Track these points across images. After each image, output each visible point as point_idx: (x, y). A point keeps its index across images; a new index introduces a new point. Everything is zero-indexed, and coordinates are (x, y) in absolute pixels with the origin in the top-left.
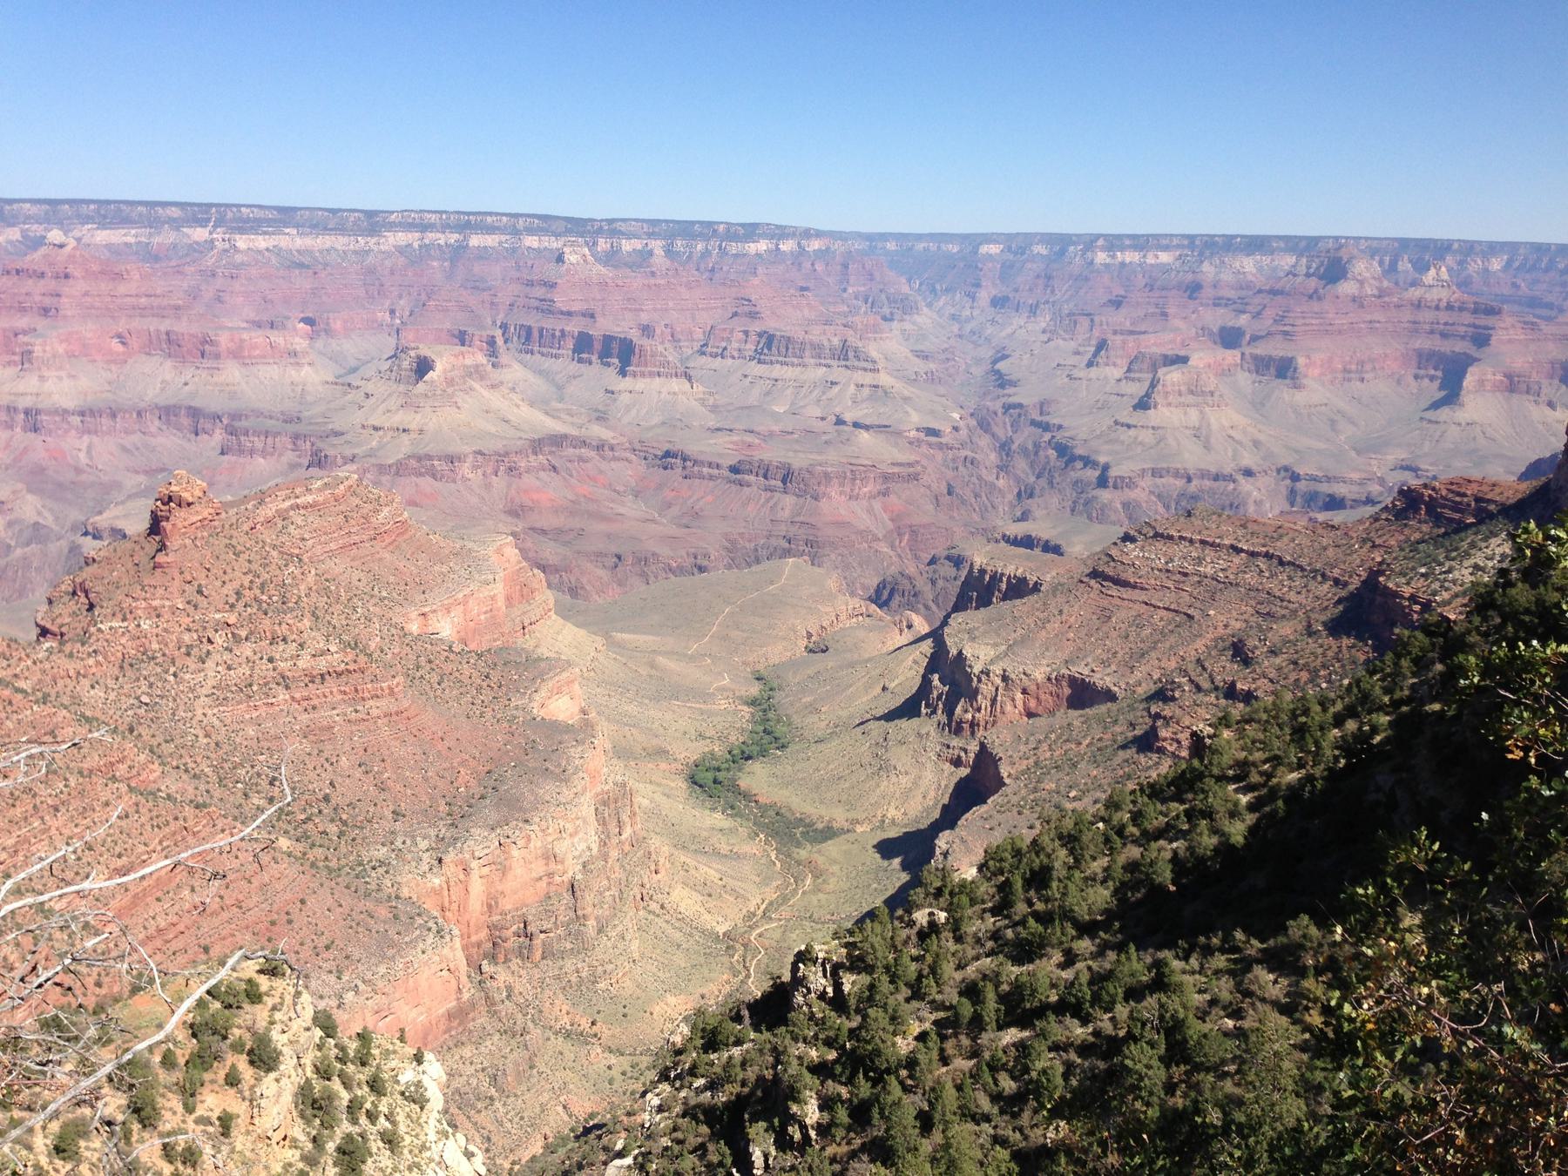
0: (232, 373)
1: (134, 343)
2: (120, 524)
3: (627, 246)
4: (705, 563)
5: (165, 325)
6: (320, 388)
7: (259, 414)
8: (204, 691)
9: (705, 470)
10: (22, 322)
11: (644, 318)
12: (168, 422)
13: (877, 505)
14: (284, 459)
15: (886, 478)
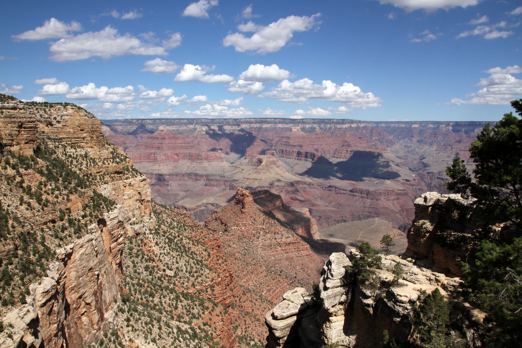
0: (206, 164)
1: (180, 156)
2: (184, 205)
3: (307, 126)
4: (346, 219)
5: (188, 151)
6: (228, 168)
7: (213, 175)
8: (259, 246)
9: (342, 191)
10: (153, 151)
11: (316, 147)
12: (189, 178)
13: (395, 202)
14: (222, 188)
15: (398, 194)
